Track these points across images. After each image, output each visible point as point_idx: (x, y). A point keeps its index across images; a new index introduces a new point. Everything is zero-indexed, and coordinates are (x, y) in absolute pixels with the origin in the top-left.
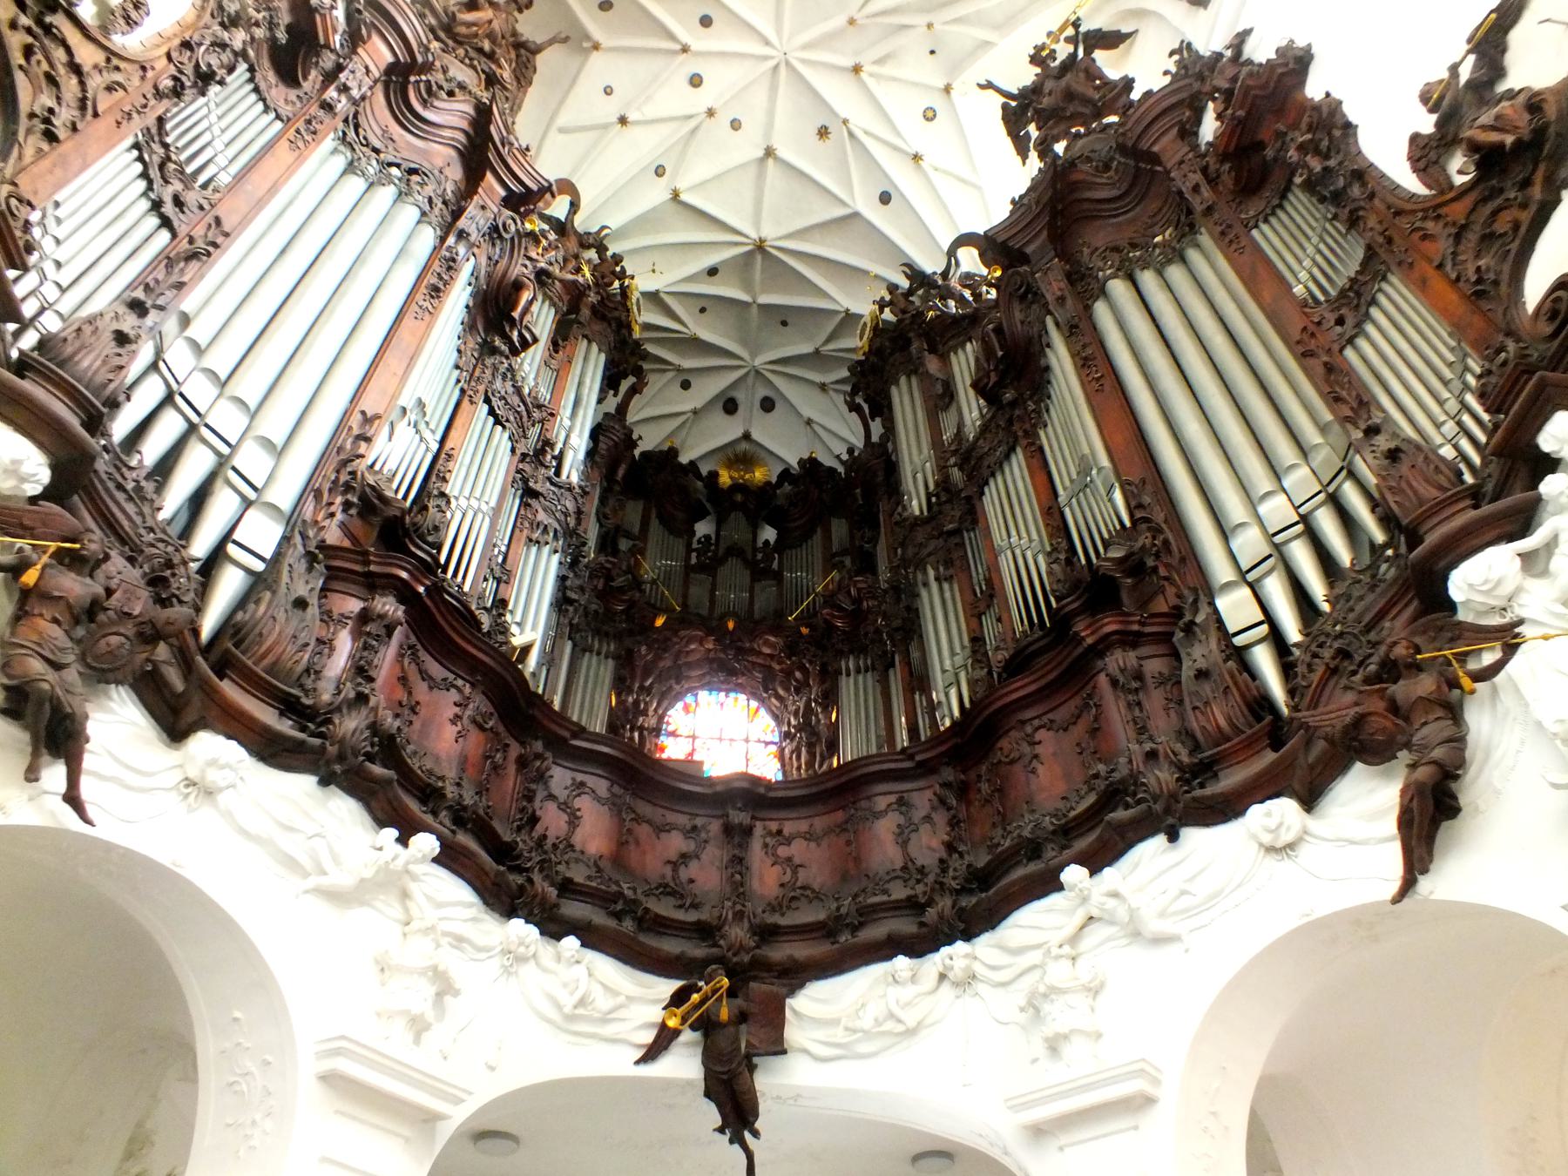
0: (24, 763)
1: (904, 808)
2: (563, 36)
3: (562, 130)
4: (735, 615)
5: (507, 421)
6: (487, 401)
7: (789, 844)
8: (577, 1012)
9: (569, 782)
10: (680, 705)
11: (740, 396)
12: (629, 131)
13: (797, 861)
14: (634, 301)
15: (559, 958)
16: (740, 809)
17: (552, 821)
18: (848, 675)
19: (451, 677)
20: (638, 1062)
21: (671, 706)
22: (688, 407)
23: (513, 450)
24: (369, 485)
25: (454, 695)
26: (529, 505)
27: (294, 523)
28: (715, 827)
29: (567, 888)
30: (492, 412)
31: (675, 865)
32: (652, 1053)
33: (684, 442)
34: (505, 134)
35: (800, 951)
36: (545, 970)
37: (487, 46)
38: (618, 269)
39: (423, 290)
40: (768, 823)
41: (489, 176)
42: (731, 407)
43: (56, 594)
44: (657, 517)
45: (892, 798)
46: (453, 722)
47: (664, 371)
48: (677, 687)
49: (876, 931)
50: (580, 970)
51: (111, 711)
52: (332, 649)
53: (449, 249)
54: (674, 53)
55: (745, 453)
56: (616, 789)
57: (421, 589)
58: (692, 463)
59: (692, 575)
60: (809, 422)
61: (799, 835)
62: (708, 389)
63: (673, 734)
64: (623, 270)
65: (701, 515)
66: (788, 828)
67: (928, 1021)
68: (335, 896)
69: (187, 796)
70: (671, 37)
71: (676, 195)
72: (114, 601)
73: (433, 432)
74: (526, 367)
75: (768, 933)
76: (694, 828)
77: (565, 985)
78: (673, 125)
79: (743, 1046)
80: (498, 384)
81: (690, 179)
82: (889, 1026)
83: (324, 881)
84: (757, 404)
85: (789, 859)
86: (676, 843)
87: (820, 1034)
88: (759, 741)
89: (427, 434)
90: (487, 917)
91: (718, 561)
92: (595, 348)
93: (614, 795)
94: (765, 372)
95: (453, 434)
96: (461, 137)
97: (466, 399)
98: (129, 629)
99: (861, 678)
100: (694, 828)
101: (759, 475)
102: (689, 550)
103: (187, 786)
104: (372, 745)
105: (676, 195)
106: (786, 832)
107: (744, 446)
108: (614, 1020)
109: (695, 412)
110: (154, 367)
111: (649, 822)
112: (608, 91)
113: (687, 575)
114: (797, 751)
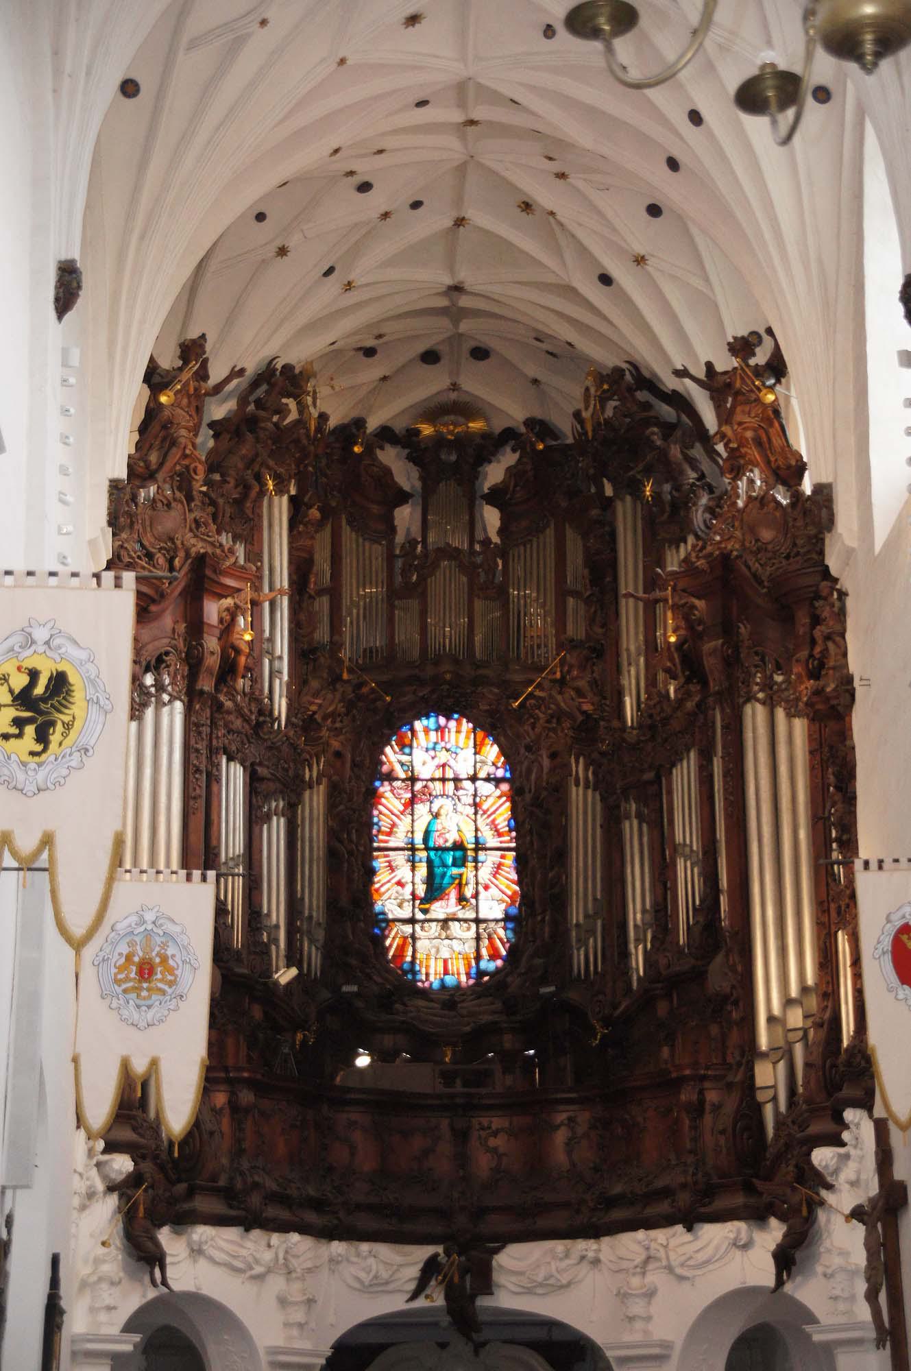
1: (572, 1124)
2: (236, 369)
4: (456, 661)
7: (495, 1134)
10: (394, 738)
11: (444, 349)
13: (501, 1150)
15: (358, 1255)
18: (577, 785)
21: (388, 743)
22: (379, 372)
23: (244, 771)
26: (259, 793)
28: (445, 1123)
32: (415, 1296)
36: (353, 1263)
39: (191, 776)
42: (430, 357)
44: (349, 523)
45: (564, 1116)
48: (390, 732)
49: (542, 1223)
55: (455, 403)
58: (386, 434)
59: (396, 602)
60: (535, 381)
63: (390, 777)
65: (403, 497)
66: (497, 1122)
67: (574, 1281)
68: (260, 1278)
77: (363, 1269)
79: (468, 1287)
82: (551, 1281)
83: (254, 1272)
85: (495, 1150)
87: (513, 1279)
88: (488, 779)
95: (215, 828)
97: (213, 778)
99: (590, 792)
101: (476, 426)
102: (390, 558)
107: (453, 396)
108: (392, 1281)
109: (385, 378)
113: (392, 607)
114: (531, 831)
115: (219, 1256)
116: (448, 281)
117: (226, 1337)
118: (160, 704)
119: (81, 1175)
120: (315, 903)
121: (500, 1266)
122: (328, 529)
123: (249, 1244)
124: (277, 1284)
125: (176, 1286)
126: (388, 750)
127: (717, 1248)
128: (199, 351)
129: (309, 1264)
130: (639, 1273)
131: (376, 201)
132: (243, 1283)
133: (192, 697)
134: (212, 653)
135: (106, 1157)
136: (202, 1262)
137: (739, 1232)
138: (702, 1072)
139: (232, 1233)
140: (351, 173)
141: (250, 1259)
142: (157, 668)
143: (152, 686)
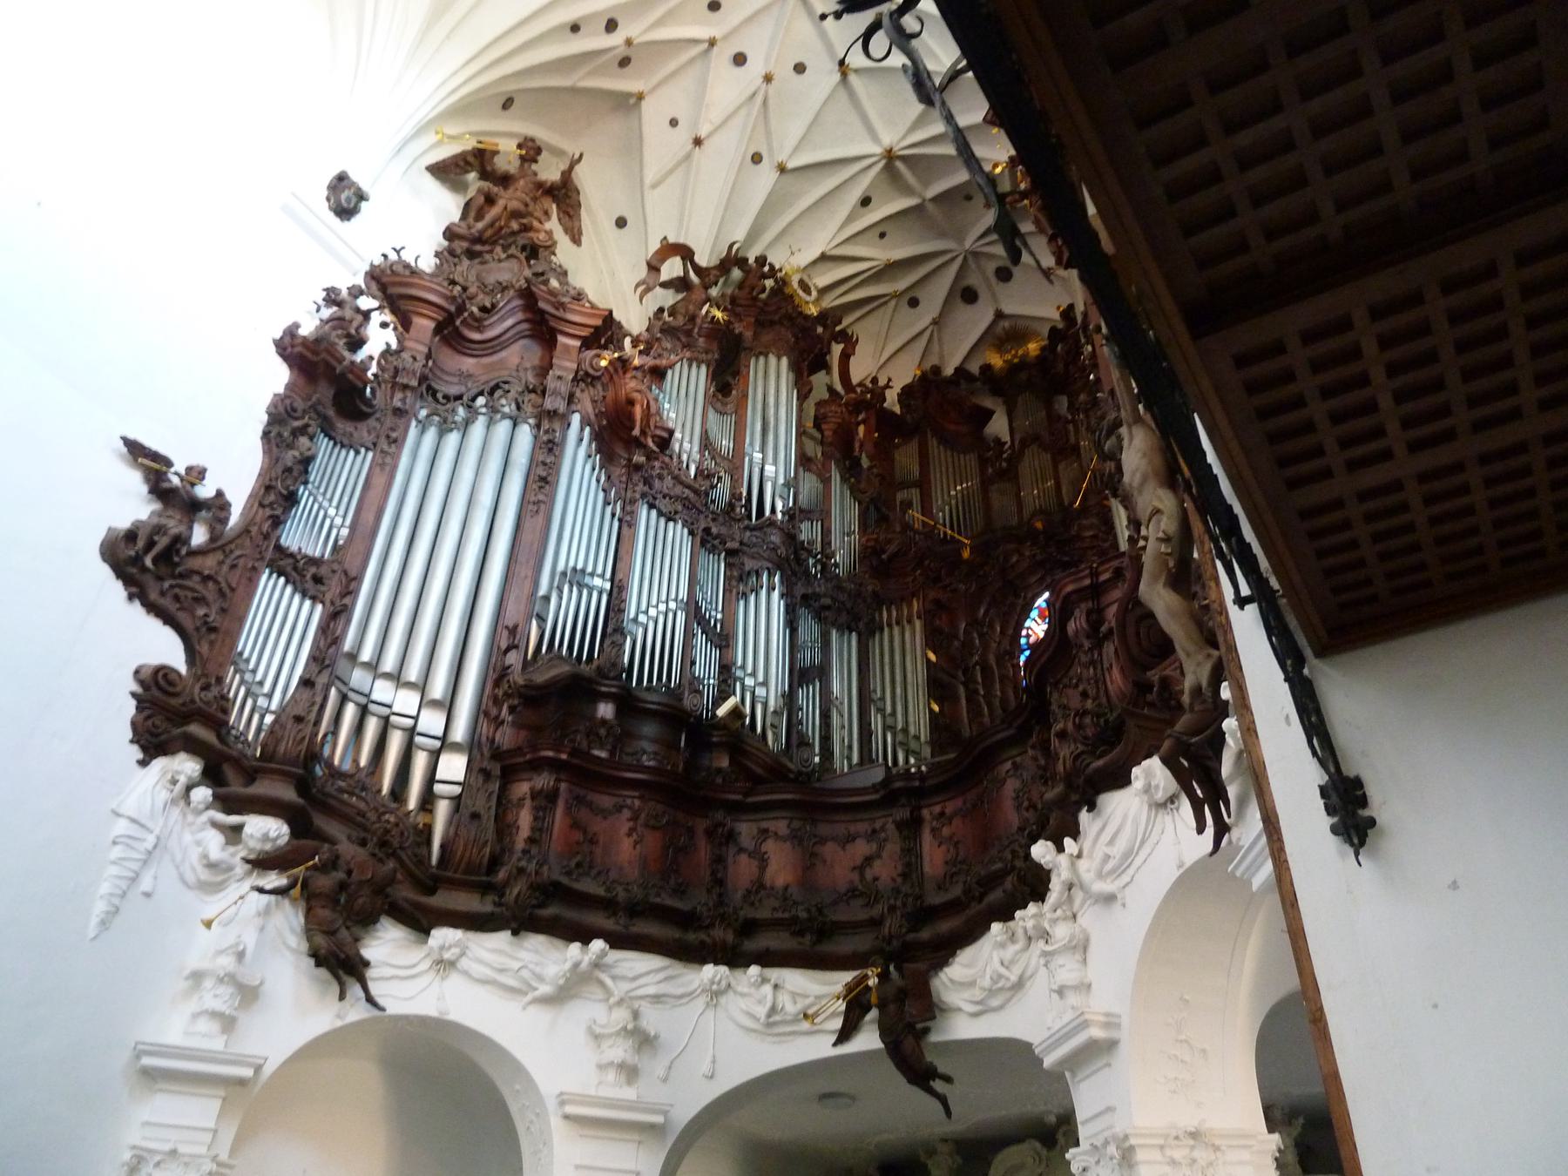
0: (336, 988)
2: (576, 156)
3: (654, 186)
5: (676, 513)
6: (651, 506)
8: (771, 1020)
9: (755, 831)
11: (973, 280)
12: (706, 144)
14: (795, 285)
16: (903, 806)
17: (742, 870)
19: (621, 799)
20: (835, 1044)
22: (927, 321)
23: (691, 533)
24: (522, 686)
25: (626, 813)
27: (472, 746)
29: (749, 928)
30: (660, 514)
31: (861, 869)
32: (844, 1035)
33: (942, 357)
34: (553, 299)
35: (945, 926)
36: (743, 995)
37: (515, 226)
38: (766, 269)
40: (932, 808)
41: (561, 339)
42: (970, 296)
43: (318, 891)
46: (629, 835)
47: (886, 303)
50: (767, 989)
51: (379, 938)
52: (518, 827)
53: (547, 432)
54: (707, 51)
56: (796, 824)
57: (564, 756)
58: (960, 371)
61: (955, 814)
62: (935, 296)
64: (771, 266)
65: (989, 414)
66: (950, 807)
68: (546, 1001)
69: (439, 970)
70: (696, 41)
71: (782, 169)
72: (355, 876)
73: (602, 576)
74: (686, 446)
75: (926, 915)
76: (874, 831)
78: (743, 112)
80: (657, 483)
81: (787, 146)
83: (537, 993)
84: (993, 280)
85: (951, 838)
86: (862, 848)
87: (967, 994)
89: (597, 582)
90: (685, 971)
91: (1016, 458)
92: (772, 359)
93: (793, 830)
94: (979, 250)
96: (525, 326)
98: (366, 891)
100: (874, 831)
101: (1033, 348)
103: (437, 964)
104: (536, 898)
105: (782, 169)
106: (948, 811)
107: (1006, 324)
109: (935, 322)
110: (344, 699)
111: (833, 839)
112: (674, 123)
115: (479, 970)
116: (878, 150)
117: (517, 1087)
118: (490, 423)
119: (134, 821)
120: (911, 719)
121: (951, 980)
122: (913, 447)
123: (523, 954)
124: (589, 1011)
125: (393, 1007)
126: (1028, 623)
127: (1136, 822)
128: (530, 144)
129: (651, 990)
130: (1065, 919)
131: (755, 68)
132: (524, 1008)
133: (549, 427)
134: (560, 378)
135: (234, 819)
136: (455, 980)
137: (1149, 774)
138: (1087, 582)
139: (502, 939)
140: (712, 43)
141: (525, 974)
142: (491, 393)
143: (481, 406)
